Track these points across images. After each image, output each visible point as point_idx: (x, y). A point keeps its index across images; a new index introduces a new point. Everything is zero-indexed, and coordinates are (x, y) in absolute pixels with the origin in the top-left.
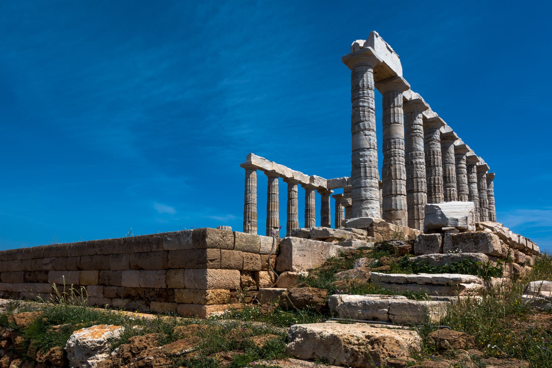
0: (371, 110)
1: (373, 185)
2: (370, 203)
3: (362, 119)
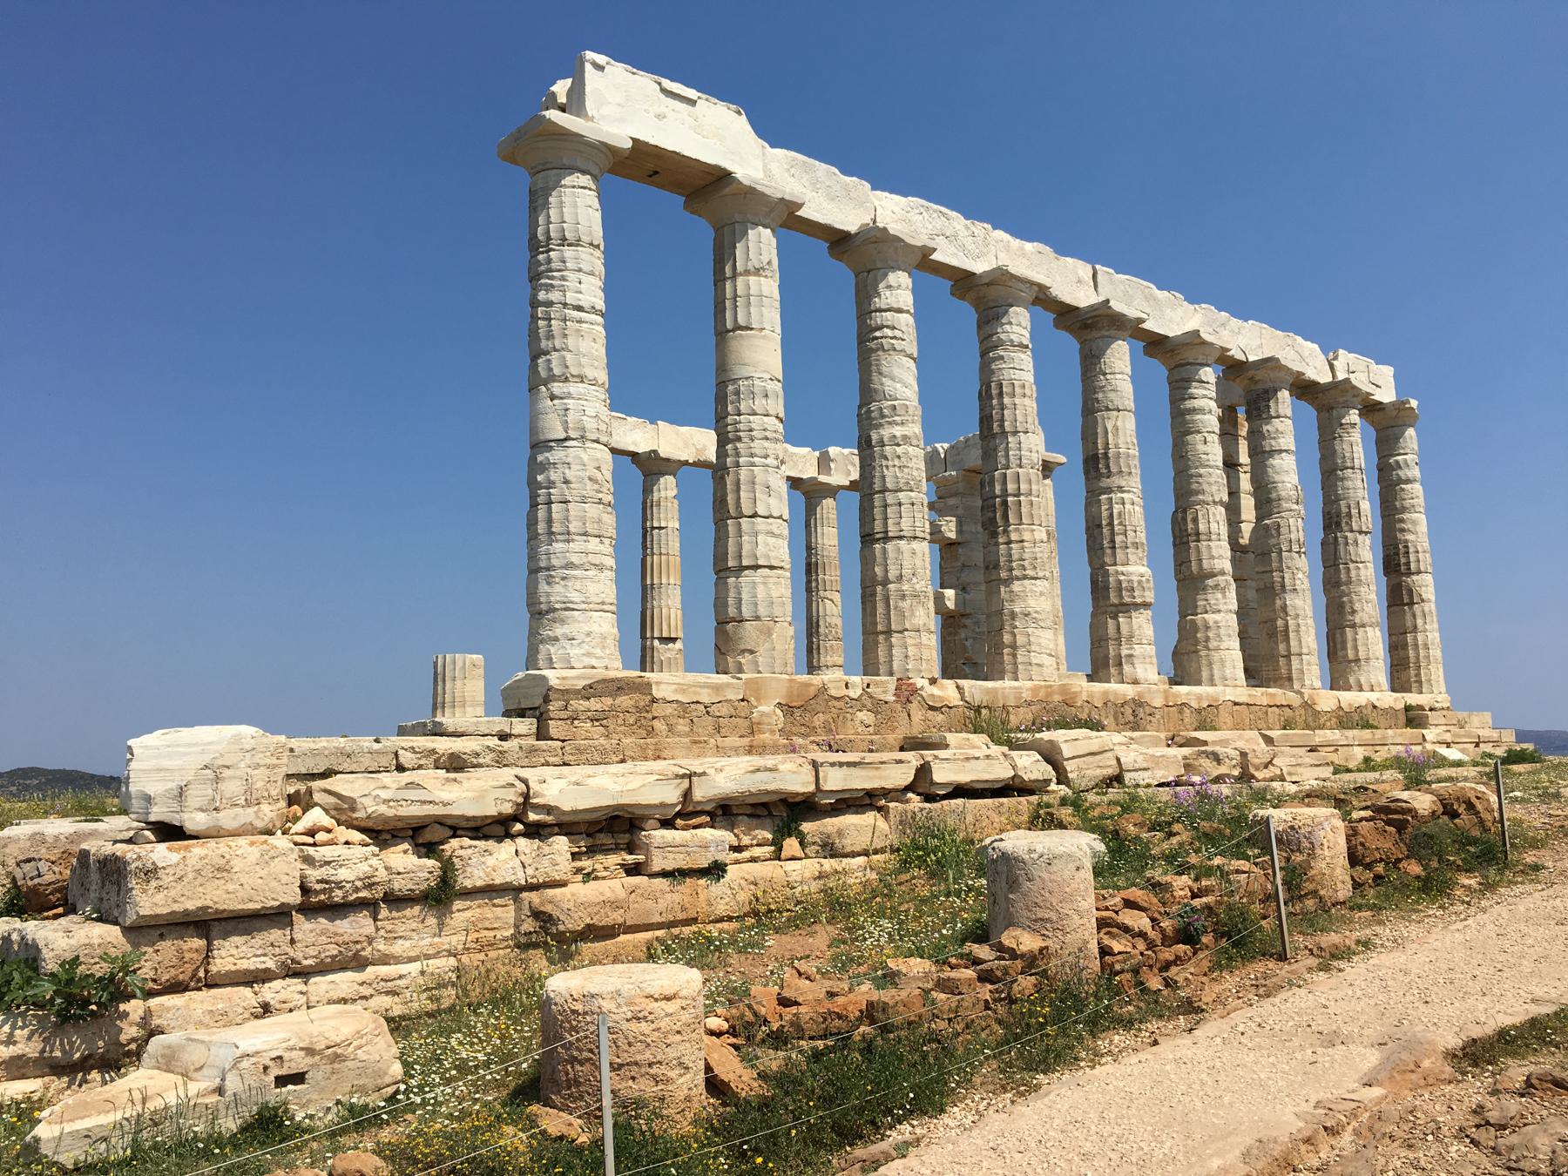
1: (575, 559)
2: (563, 621)
3: (543, 344)
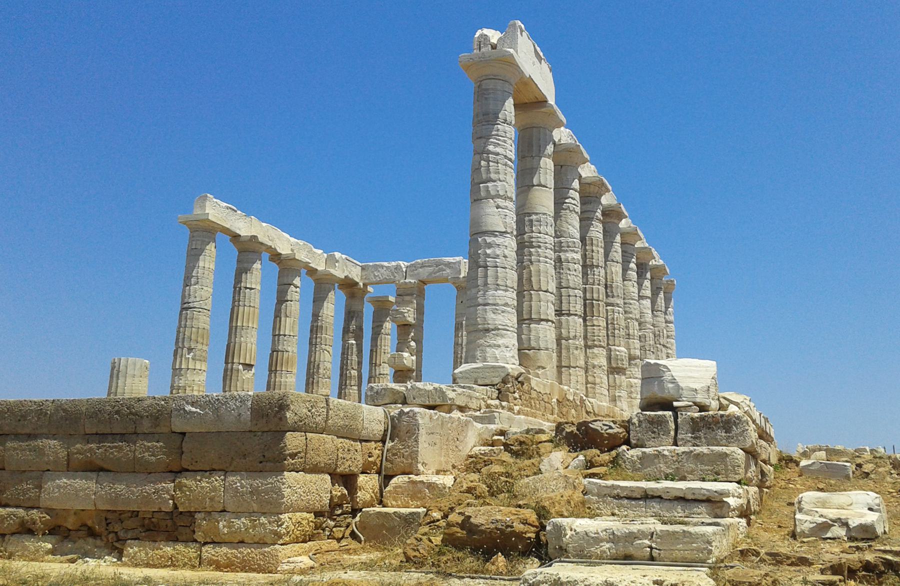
0: (509, 163)
2: (502, 336)
3: (493, 176)
